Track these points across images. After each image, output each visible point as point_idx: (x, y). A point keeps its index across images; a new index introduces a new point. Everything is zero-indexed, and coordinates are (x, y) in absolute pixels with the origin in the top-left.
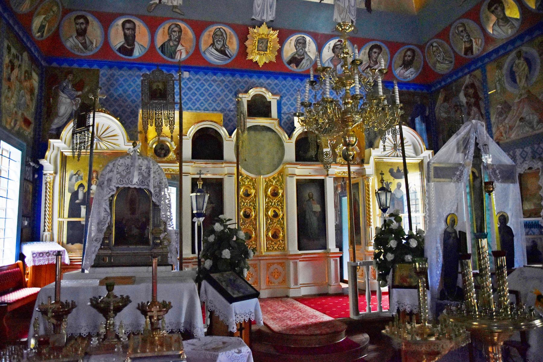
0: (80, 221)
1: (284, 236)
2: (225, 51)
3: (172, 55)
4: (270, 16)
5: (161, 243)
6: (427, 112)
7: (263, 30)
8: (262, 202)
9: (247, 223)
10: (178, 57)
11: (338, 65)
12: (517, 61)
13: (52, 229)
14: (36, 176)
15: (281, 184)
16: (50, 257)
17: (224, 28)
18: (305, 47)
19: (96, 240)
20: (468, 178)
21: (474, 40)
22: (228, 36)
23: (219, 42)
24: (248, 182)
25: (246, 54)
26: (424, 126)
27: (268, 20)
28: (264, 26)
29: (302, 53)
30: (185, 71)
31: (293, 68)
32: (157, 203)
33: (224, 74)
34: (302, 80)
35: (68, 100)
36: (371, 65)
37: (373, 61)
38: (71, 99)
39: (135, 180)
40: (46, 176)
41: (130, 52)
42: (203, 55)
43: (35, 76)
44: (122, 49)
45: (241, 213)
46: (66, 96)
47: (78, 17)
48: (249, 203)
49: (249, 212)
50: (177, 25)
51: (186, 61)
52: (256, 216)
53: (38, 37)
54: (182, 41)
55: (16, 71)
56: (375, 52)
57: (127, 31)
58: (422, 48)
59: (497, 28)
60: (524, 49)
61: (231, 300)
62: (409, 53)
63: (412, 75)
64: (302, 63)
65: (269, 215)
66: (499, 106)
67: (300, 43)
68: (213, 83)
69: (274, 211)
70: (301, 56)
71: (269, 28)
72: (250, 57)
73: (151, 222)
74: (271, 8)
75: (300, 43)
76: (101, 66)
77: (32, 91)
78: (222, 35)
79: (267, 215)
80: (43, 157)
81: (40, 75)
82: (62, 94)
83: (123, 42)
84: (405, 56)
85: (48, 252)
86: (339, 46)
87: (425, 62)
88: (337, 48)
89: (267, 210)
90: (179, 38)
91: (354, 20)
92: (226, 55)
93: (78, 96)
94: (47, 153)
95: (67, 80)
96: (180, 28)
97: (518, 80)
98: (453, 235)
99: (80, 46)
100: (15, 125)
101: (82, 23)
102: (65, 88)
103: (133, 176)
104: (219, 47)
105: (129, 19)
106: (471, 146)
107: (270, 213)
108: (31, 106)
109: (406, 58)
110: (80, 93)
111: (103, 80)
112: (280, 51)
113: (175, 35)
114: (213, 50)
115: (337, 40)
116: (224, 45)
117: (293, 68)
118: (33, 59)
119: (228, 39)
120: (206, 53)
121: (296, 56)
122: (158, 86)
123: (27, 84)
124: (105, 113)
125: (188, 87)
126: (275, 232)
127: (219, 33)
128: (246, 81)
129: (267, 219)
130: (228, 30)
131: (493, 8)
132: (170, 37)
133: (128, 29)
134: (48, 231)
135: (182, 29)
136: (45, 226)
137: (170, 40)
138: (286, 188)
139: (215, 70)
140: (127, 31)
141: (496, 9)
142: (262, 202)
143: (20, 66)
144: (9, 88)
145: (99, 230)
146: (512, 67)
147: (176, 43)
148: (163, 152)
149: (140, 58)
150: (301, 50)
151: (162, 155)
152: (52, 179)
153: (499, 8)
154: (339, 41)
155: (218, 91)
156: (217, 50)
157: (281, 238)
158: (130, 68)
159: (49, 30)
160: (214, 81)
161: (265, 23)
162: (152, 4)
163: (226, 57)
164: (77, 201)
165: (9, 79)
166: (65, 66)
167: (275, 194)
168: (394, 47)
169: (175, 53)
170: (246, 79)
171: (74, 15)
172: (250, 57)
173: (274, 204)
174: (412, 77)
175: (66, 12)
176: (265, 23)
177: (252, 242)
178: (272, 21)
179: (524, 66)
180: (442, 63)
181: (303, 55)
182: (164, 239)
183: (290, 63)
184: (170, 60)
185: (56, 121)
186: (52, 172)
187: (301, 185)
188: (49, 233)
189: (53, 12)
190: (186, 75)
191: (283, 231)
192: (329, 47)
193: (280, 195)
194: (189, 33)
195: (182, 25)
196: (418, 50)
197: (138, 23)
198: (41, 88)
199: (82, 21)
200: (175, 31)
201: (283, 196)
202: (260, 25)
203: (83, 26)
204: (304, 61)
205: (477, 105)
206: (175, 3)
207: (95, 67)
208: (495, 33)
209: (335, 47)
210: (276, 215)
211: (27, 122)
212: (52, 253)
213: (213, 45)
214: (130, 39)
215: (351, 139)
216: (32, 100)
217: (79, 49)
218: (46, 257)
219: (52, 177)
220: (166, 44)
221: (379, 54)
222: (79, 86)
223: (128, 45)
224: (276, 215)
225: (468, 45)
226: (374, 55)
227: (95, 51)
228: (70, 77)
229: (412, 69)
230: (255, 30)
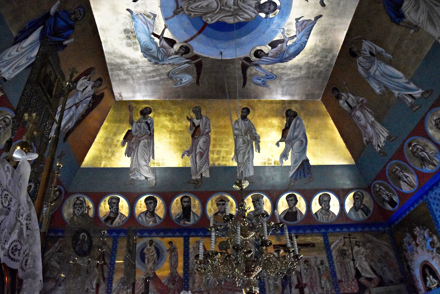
12: (148, 247)
59: (143, 216)
67: (5, 121)
74: (16, 68)
75: (5, 121)
97: (146, 261)
131: (148, 202)
141: (151, 203)
146: (143, 249)
153: (153, 204)
178: (5, 79)
179: (153, 253)
208: (140, 218)
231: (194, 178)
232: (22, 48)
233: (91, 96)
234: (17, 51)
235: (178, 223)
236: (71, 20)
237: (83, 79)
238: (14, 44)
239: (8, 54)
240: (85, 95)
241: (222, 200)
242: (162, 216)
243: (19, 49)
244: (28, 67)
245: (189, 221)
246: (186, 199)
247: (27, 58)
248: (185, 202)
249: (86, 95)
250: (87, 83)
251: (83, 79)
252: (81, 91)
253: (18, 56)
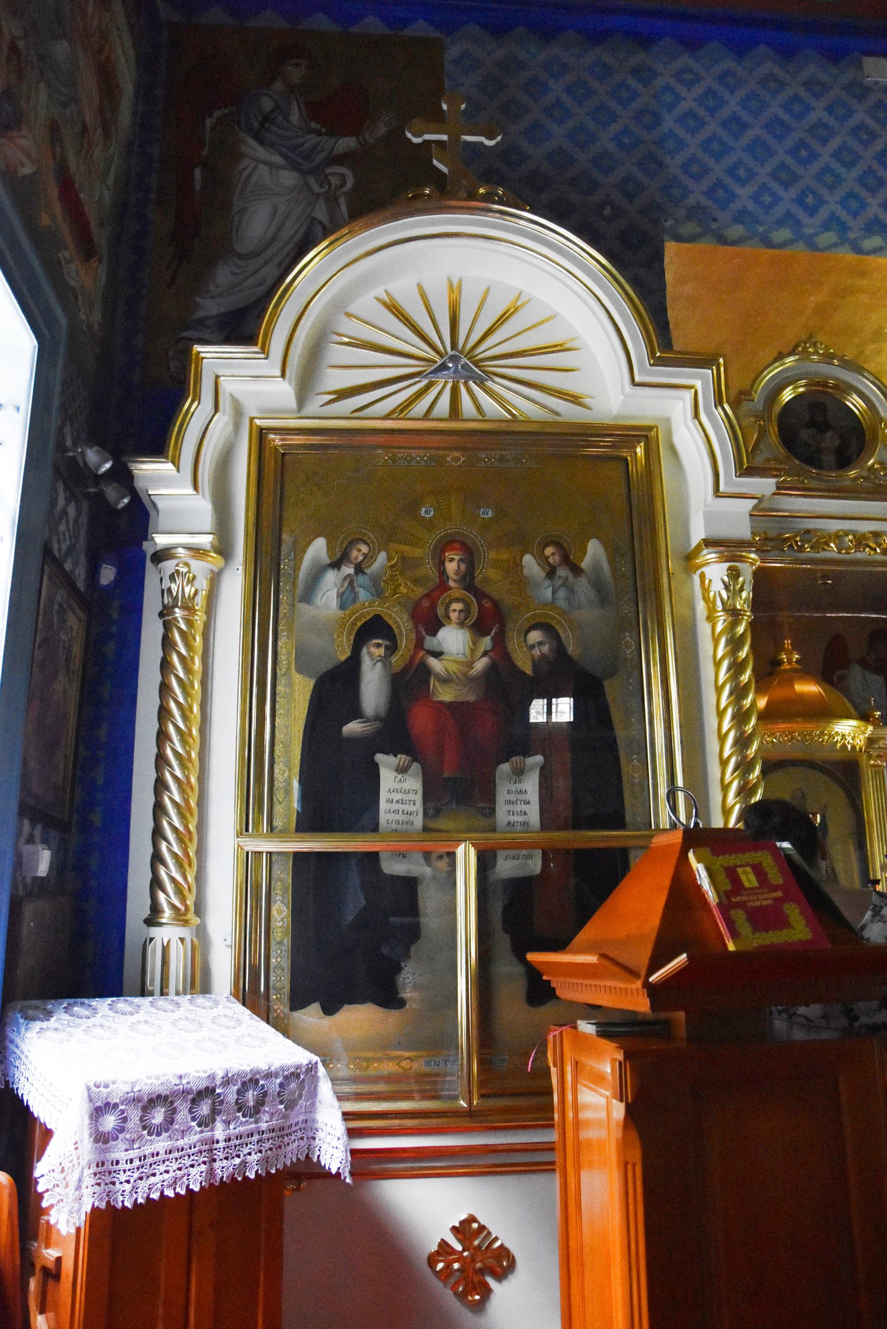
0: (373, 858)
13: (200, 909)
14: (108, 574)
16: (219, 1132)
35: (289, 178)
38: (304, 173)
40: (169, 566)
46: (277, 159)
82: (252, 147)
85: (208, 1092)
93: (340, 160)
95: (278, 85)
102: (267, 118)
110: (346, 143)
134: (180, 917)
136: (156, 884)
148: (830, 440)
151: (829, 459)
152: (203, 584)
164: (353, 728)
185: (223, 276)
186: (206, 540)
188: (184, 932)
212: (231, 1094)
219: (200, 568)
228: (295, 73)
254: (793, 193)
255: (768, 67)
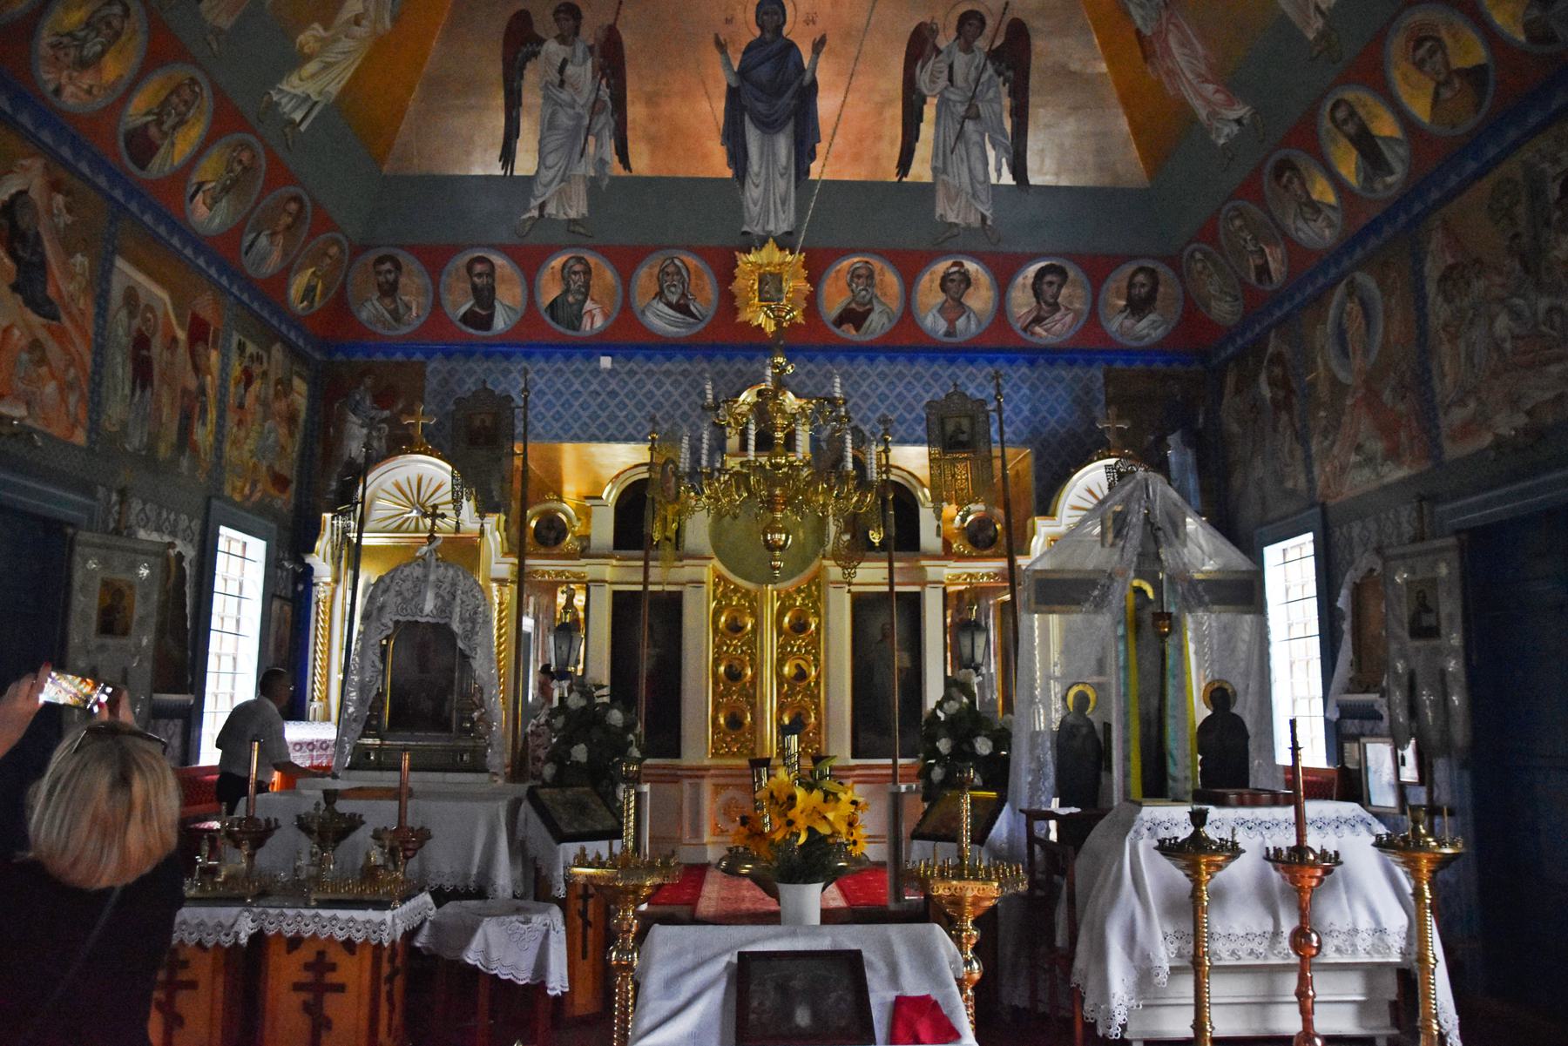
1: (819, 724)
2: (688, 306)
3: (575, 321)
4: (782, 222)
5: (472, 729)
6: (1201, 420)
7: (769, 255)
8: (770, 643)
9: (799, 692)
10: (586, 324)
11: (957, 319)
13: (327, 697)
14: (301, 587)
15: (815, 603)
16: (315, 753)
17: (684, 257)
18: (872, 285)
19: (355, 720)
20: (1123, 604)
21: (1267, 251)
22: (693, 277)
23: (673, 289)
24: (739, 599)
25: (736, 311)
26: (1190, 457)
27: (780, 232)
28: (771, 246)
29: (868, 297)
30: (604, 355)
31: (849, 333)
32: (468, 652)
33: (690, 358)
34: (872, 360)
36: (1042, 313)
37: (1046, 302)
39: (429, 605)
41: (486, 322)
42: (639, 316)
43: (300, 386)
44: (469, 319)
45: (722, 669)
47: (381, 261)
48: (742, 645)
49: (739, 668)
50: (580, 260)
51: (602, 334)
52: (754, 676)
53: (303, 309)
54: (594, 291)
55: (256, 386)
56: (1051, 283)
57: (476, 279)
58: (1173, 262)
60: (1361, 277)
61: (562, 838)
62: (1141, 278)
63: (1156, 329)
64: (867, 323)
65: (783, 676)
66: (1322, 414)
67: (859, 277)
68: (663, 378)
69: (798, 666)
70: (865, 305)
71: (782, 249)
72: (745, 316)
73: (456, 688)
74: (783, 203)
75: (859, 277)
76: (429, 355)
77: (291, 419)
78: (679, 272)
79: (780, 675)
80: (310, 549)
81: (313, 384)
83: (472, 303)
84: (1131, 285)
85: (309, 744)
86: (955, 277)
87: (1187, 298)
88: (952, 281)
89: (781, 663)
90: (587, 286)
91: (988, 214)
92: (692, 315)
93: (383, 421)
94: (318, 544)
96: (587, 264)
98: (1084, 730)
99: (387, 315)
100: (252, 492)
101: (389, 271)
103: (424, 600)
104: (674, 299)
105: (476, 255)
106: (1131, 533)
107: (786, 670)
108: (289, 450)
109: (1136, 291)
110: (387, 413)
111: (432, 383)
112: (812, 301)
113: (578, 280)
114: (662, 307)
115: (950, 262)
116: (684, 295)
117: (849, 333)
118: (292, 350)
119: (693, 281)
120: (648, 314)
121: (853, 305)
122: (483, 421)
123: (280, 406)
124: (431, 455)
125: (608, 389)
126: (799, 715)
127: (671, 269)
128: (739, 370)
129: (780, 685)
130: (692, 261)
132: (568, 284)
133: (480, 275)
134: (320, 699)
135: (592, 266)
136: (313, 690)
137: (567, 291)
138: (827, 613)
139: (666, 348)
140: (476, 279)
141: (1290, 181)
142: (770, 643)
143: (265, 374)
144: (240, 423)
145: (361, 701)
146: (1341, 317)
147: (580, 297)
149: (501, 336)
150: (864, 293)
151: (551, 542)
152: (329, 593)
154: (954, 264)
155: (676, 395)
156: (669, 305)
157: (810, 728)
158: (488, 356)
159: (324, 294)
160: (668, 373)
161: (771, 240)
162: (525, 221)
163: (692, 320)
165: (241, 406)
166: (359, 357)
167: (800, 627)
168: (1097, 269)
169: (579, 317)
170: (739, 364)
171: (372, 256)
172: (745, 316)
173: (799, 650)
174: (1158, 334)
175: (358, 250)
176: (771, 240)
177: (743, 734)
178: (789, 233)
180: (1220, 300)
181: (870, 301)
182: (480, 719)
183: (840, 321)
184: (570, 332)
186: (329, 580)
187: (863, 605)
189: (330, 257)
190: (606, 362)
191: (818, 714)
192: (932, 281)
193: (813, 627)
194: (606, 275)
195: (593, 259)
196: (1164, 271)
197: (498, 260)
198: (311, 409)
199: (387, 266)
200: (575, 273)
201: (818, 628)
202: (763, 242)
203: (391, 277)
204: (874, 317)
205: (1288, 406)
206: (573, 214)
207: (418, 357)
209: (945, 280)
210: (801, 675)
211: (280, 482)
213: (660, 295)
214: (485, 297)
215: (777, 536)
216: (291, 434)
217: (384, 323)
218: (308, 753)
219: (328, 590)
220: (559, 300)
221: (1060, 287)
222: (384, 398)
223: (483, 309)
224: (801, 675)
225: (1259, 262)
226: (1048, 292)
227: (417, 323)
228: (368, 381)
229: (1152, 317)
230: (751, 258)
231: (1311, 36)
232: (758, 175)
233: (985, 65)
234: (757, 186)
235: (1370, 195)
236: (773, 42)
237: (922, 67)
238: (743, 185)
239: (751, 206)
240: (966, 80)
241: (1419, 43)
242: (1331, 198)
243: (757, 182)
244: (796, 182)
245: (1391, 173)
246: (1341, 114)
247: (782, 175)
248: (1345, 121)
249: (973, 74)
250: (940, 62)
251: (922, 67)
252: (946, 88)
253: (766, 190)
254: (560, 424)
255: (560, 365)
